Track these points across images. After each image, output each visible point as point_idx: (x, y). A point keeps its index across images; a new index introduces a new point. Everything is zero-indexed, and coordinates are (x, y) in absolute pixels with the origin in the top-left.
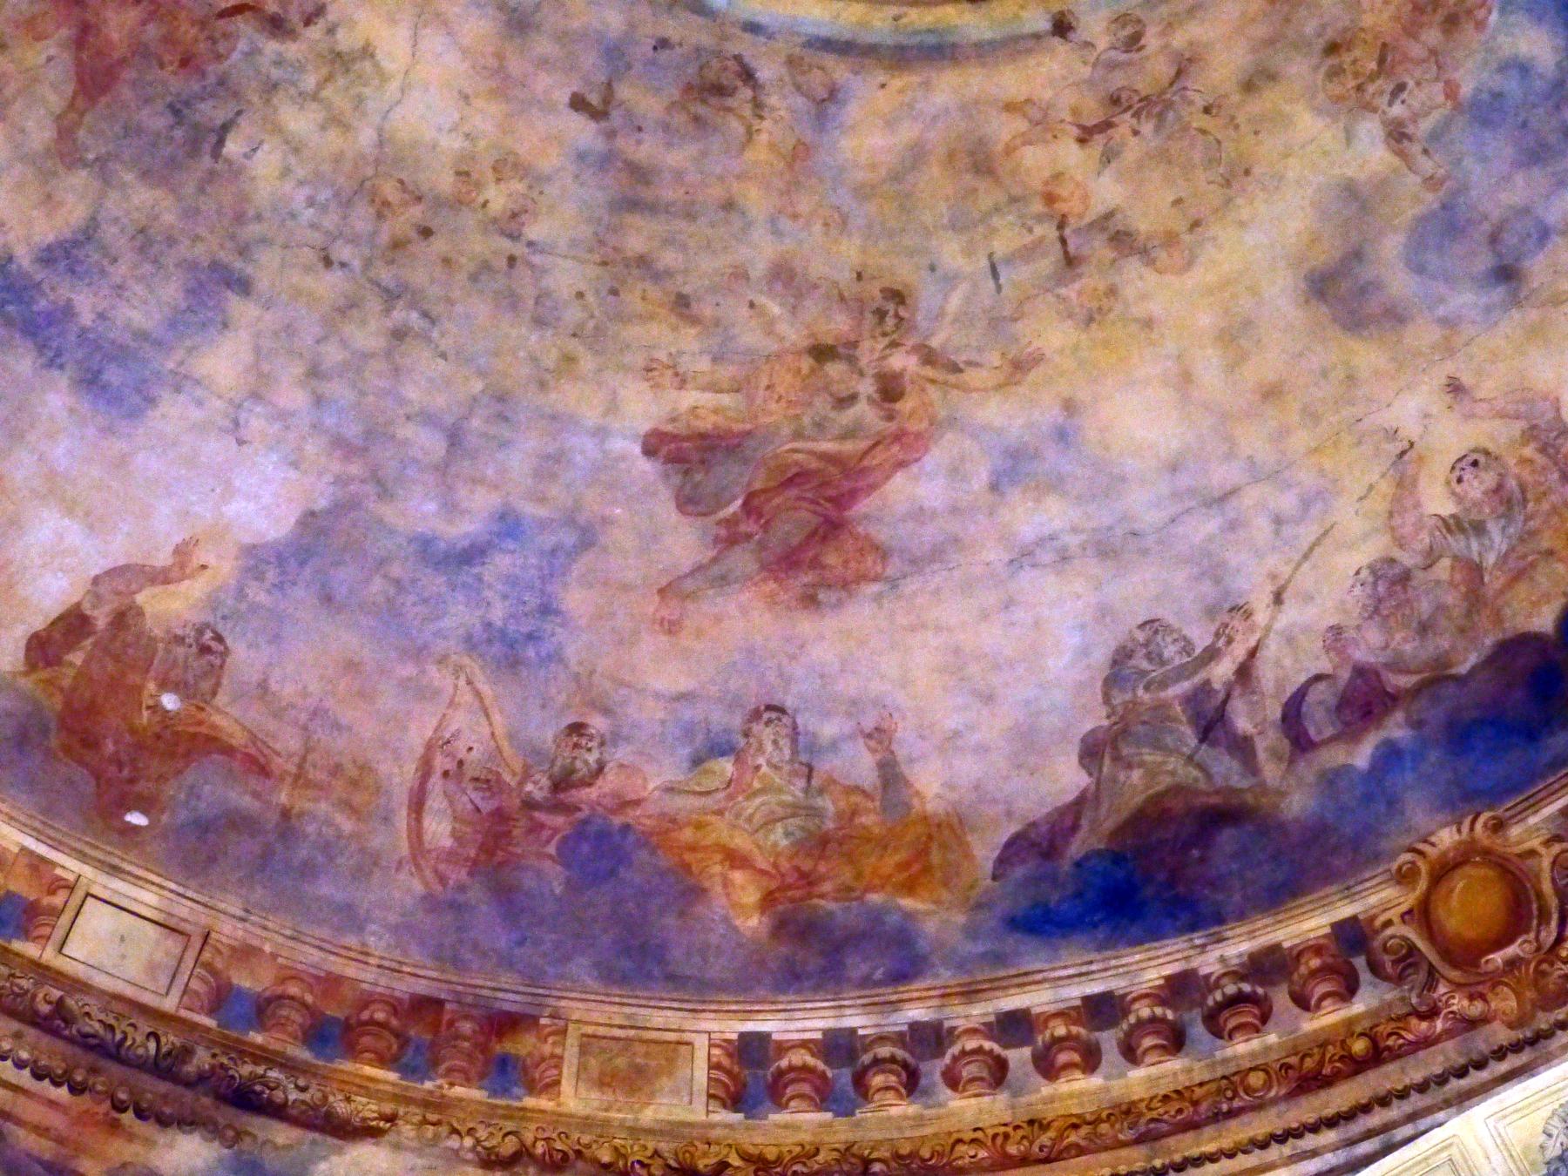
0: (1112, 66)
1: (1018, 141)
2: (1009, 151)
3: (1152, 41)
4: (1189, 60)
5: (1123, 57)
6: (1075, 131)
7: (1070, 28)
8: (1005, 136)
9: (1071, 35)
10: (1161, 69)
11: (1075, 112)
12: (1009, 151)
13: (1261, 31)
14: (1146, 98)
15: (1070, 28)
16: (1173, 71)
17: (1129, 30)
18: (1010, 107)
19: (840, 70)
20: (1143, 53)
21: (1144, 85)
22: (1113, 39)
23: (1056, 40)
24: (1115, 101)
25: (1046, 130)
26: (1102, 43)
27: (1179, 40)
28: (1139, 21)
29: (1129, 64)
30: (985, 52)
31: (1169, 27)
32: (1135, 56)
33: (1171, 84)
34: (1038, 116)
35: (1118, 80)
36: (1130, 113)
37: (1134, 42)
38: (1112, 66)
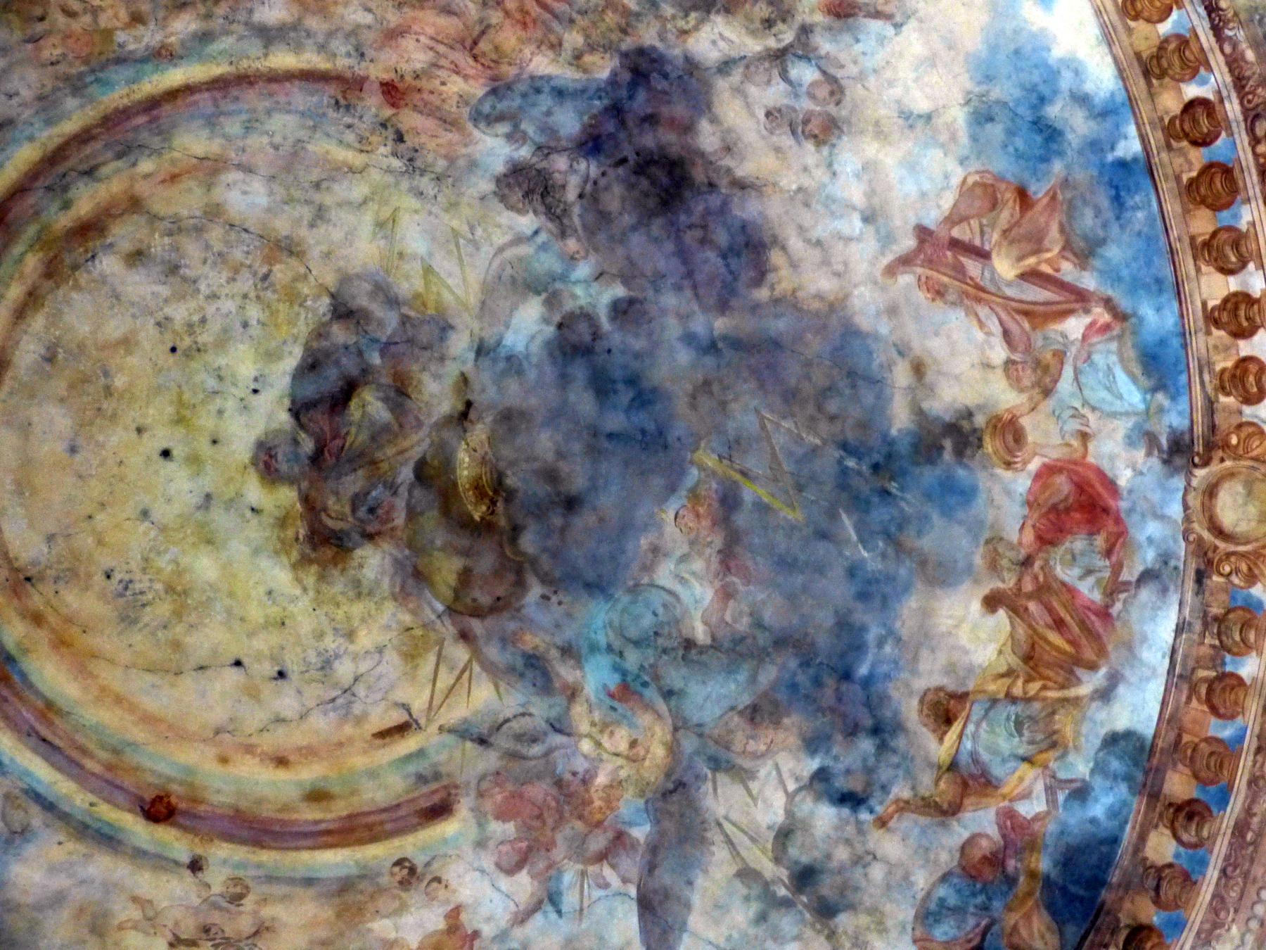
0: (216, 906)
1: (129, 925)
2: (121, 927)
3: (249, 903)
4: (267, 929)
5: (225, 905)
6: (170, 937)
7: (200, 869)
8: (122, 917)
9: (200, 875)
10: (245, 924)
11: (177, 924)
12: (121, 927)
13: (322, 933)
14: (227, 938)
15: (200, 869)
16: (253, 930)
17: (238, 890)
18: (135, 899)
19: (37, 818)
20: (241, 908)
21: (229, 932)
22: (224, 889)
23: (188, 872)
24: (206, 930)
25: (153, 926)
26: (217, 889)
27: (267, 912)
28: (247, 887)
29: (228, 911)
30: (139, 855)
31: (264, 901)
32: (232, 907)
33: (248, 938)
34: (151, 914)
35: (216, 918)
36: (210, 943)
37: (237, 899)
38: (216, 906)
